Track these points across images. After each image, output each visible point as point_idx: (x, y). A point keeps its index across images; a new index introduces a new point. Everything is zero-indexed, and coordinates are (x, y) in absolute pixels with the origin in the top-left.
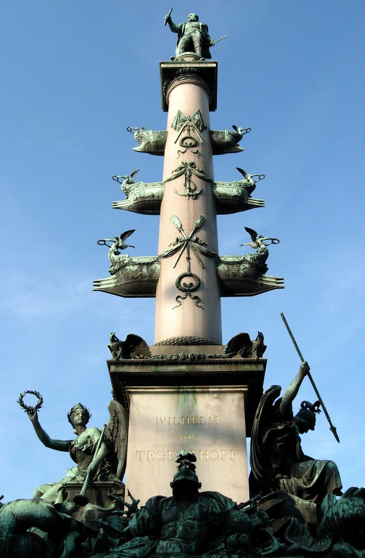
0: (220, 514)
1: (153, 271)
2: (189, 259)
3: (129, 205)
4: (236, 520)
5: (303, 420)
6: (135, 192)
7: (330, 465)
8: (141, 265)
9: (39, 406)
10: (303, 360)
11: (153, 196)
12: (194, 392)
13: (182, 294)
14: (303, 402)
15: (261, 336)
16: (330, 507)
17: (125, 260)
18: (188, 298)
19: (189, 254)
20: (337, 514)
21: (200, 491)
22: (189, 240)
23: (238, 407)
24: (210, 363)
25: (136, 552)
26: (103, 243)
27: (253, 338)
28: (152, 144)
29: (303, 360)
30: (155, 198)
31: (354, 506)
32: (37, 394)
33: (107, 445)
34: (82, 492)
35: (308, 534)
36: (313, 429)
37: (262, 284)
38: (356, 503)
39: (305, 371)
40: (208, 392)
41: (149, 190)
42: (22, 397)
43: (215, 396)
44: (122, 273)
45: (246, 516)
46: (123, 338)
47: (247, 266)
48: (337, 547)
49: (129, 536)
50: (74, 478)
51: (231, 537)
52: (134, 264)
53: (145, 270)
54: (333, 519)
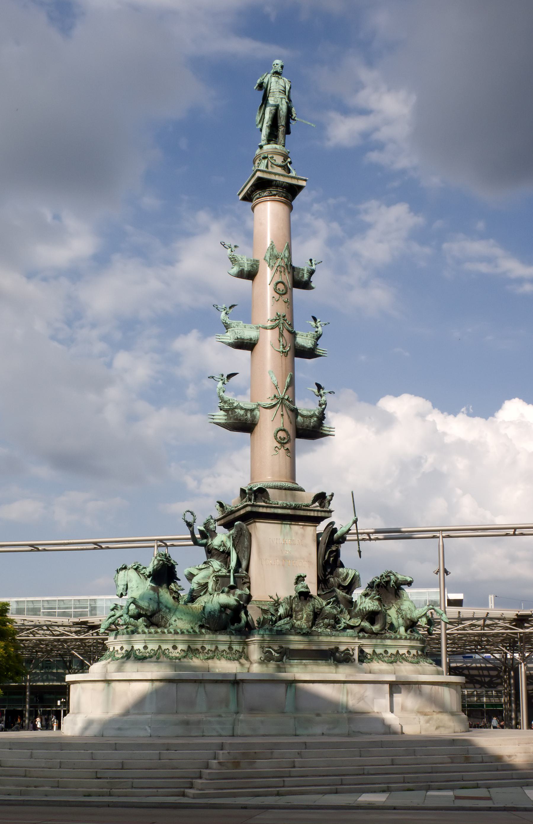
1: (254, 417)
2: (282, 415)
3: (230, 341)
6: (236, 331)
8: (246, 410)
10: (355, 516)
11: (251, 339)
13: (278, 445)
16: (361, 603)
17: (234, 403)
18: (282, 449)
22: (283, 399)
24: (304, 510)
28: (245, 272)
29: (355, 516)
30: (253, 342)
31: (374, 605)
34: (232, 583)
37: (322, 433)
38: (375, 604)
41: (249, 334)
43: (301, 527)
44: (232, 414)
49: (280, 618)
50: (220, 570)
52: (242, 408)
53: (249, 415)
54: (363, 610)
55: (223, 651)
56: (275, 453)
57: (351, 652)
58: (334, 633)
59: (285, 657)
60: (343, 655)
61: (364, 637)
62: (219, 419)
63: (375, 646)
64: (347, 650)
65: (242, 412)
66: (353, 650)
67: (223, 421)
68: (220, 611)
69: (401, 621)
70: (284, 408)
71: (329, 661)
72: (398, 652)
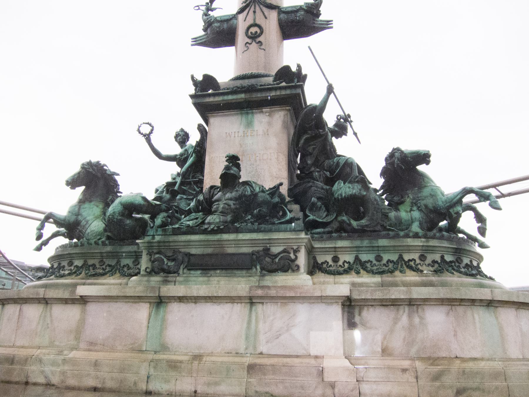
0: (250, 196)
2: (254, 12)
4: (261, 199)
5: (336, 129)
7: (350, 161)
9: (151, 132)
12: (252, 113)
13: (249, 41)
14: (338, 116)
15: (299, 66)
18: (254, 43)
19: (255, 9)
20: (341, 195)
21: (241, 181)
23: (284, 122)
25: (190, 223)
26: (198, 8)
27: (294, 69)
32: (150, 125)
33: (197, 156)
34: (176, 188)
35: (324, 209)
36: (346, 135)
37: (314, 27)
39: (330, 90)
40: (262, 112)
42: (139, 127)
43: (267, 114)
45: (268, 197)
46: (200, 78)
47: (302, 13)
48: (340, 218)
49: (189, 212)
51: (255, 211)
54: (338, 198)
55: (124, 266)
56: (246, 49)
57: (292, 256)
58: (263, 226)
59: (182, 267)
60: (277, 260)
61: (341, 238)
62: (201, 40)
63: (358, 249)
64: (284, 251)
65: (218, 24)
66: (296, 251)
67: (204, 40)
68: (122, 214)
69: (416, 214)
70: (257, 6)
71: (254, 270)
72: (401, 257)
